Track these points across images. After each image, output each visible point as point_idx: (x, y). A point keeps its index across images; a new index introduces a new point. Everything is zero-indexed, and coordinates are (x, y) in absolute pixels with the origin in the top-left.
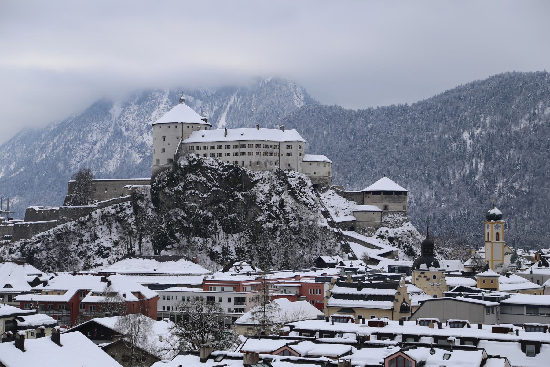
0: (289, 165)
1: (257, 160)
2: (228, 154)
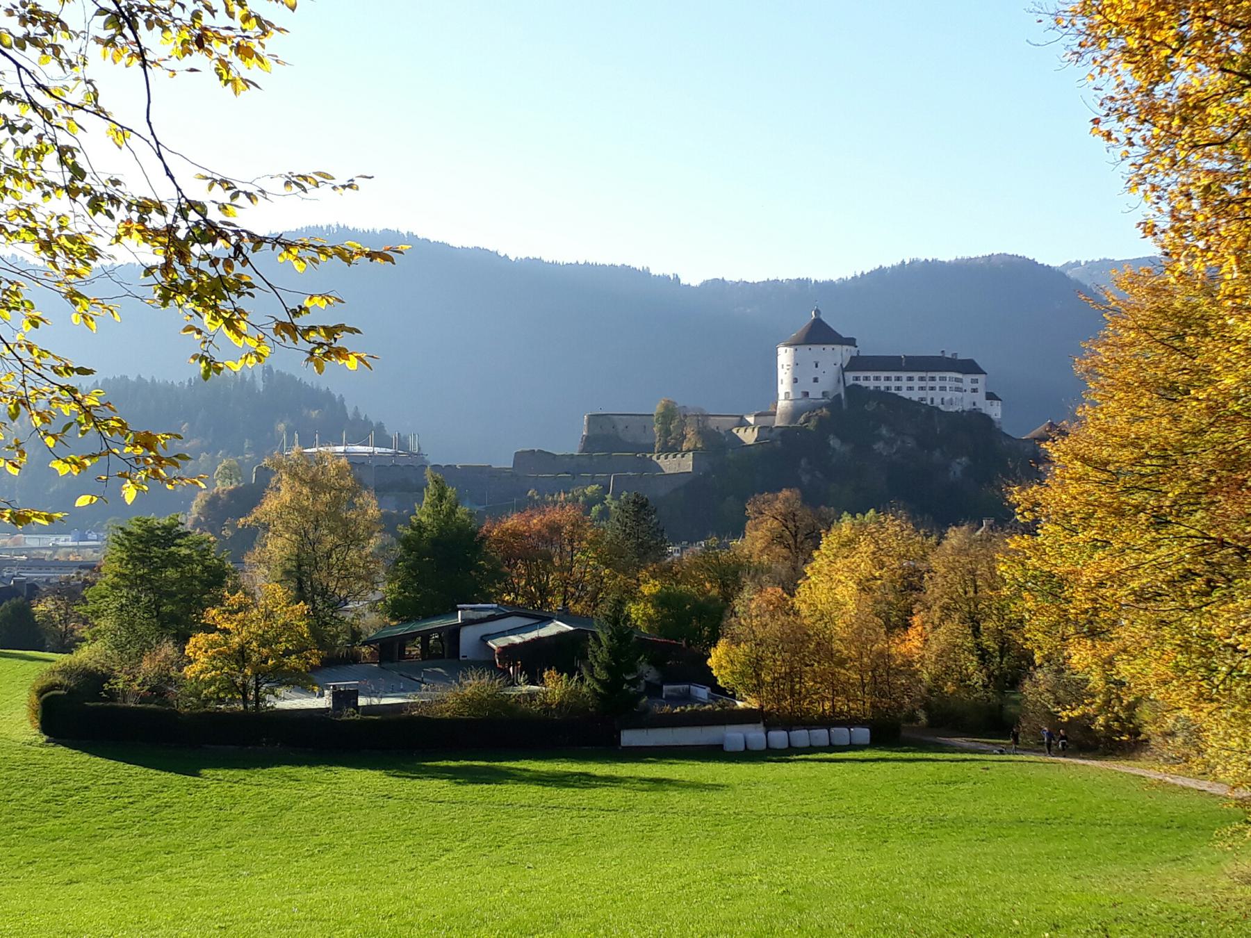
0: (974, 404)
2: (910, 388)
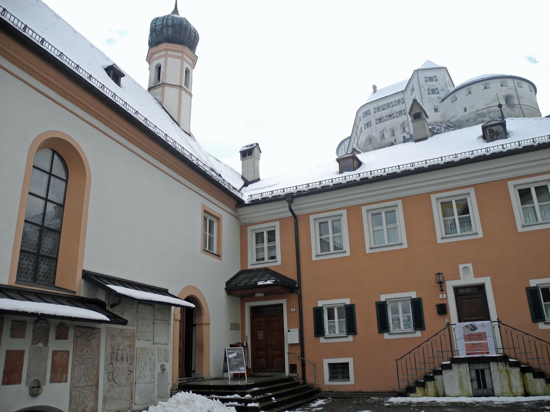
1: (367, 136)
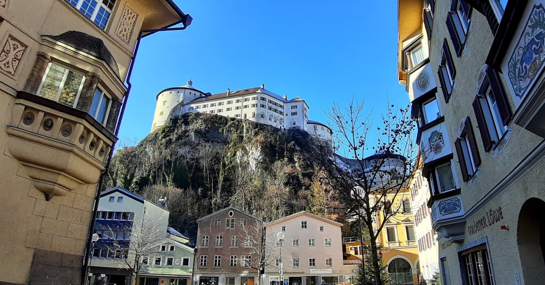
2: (228, 109)
